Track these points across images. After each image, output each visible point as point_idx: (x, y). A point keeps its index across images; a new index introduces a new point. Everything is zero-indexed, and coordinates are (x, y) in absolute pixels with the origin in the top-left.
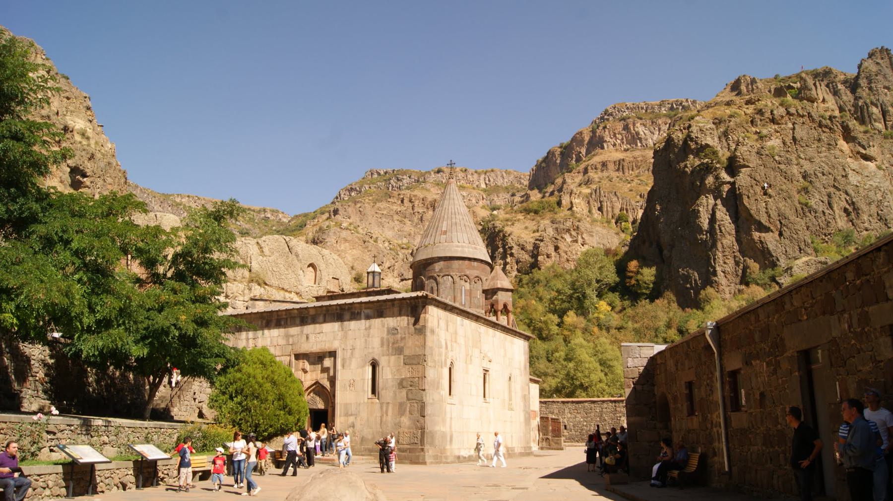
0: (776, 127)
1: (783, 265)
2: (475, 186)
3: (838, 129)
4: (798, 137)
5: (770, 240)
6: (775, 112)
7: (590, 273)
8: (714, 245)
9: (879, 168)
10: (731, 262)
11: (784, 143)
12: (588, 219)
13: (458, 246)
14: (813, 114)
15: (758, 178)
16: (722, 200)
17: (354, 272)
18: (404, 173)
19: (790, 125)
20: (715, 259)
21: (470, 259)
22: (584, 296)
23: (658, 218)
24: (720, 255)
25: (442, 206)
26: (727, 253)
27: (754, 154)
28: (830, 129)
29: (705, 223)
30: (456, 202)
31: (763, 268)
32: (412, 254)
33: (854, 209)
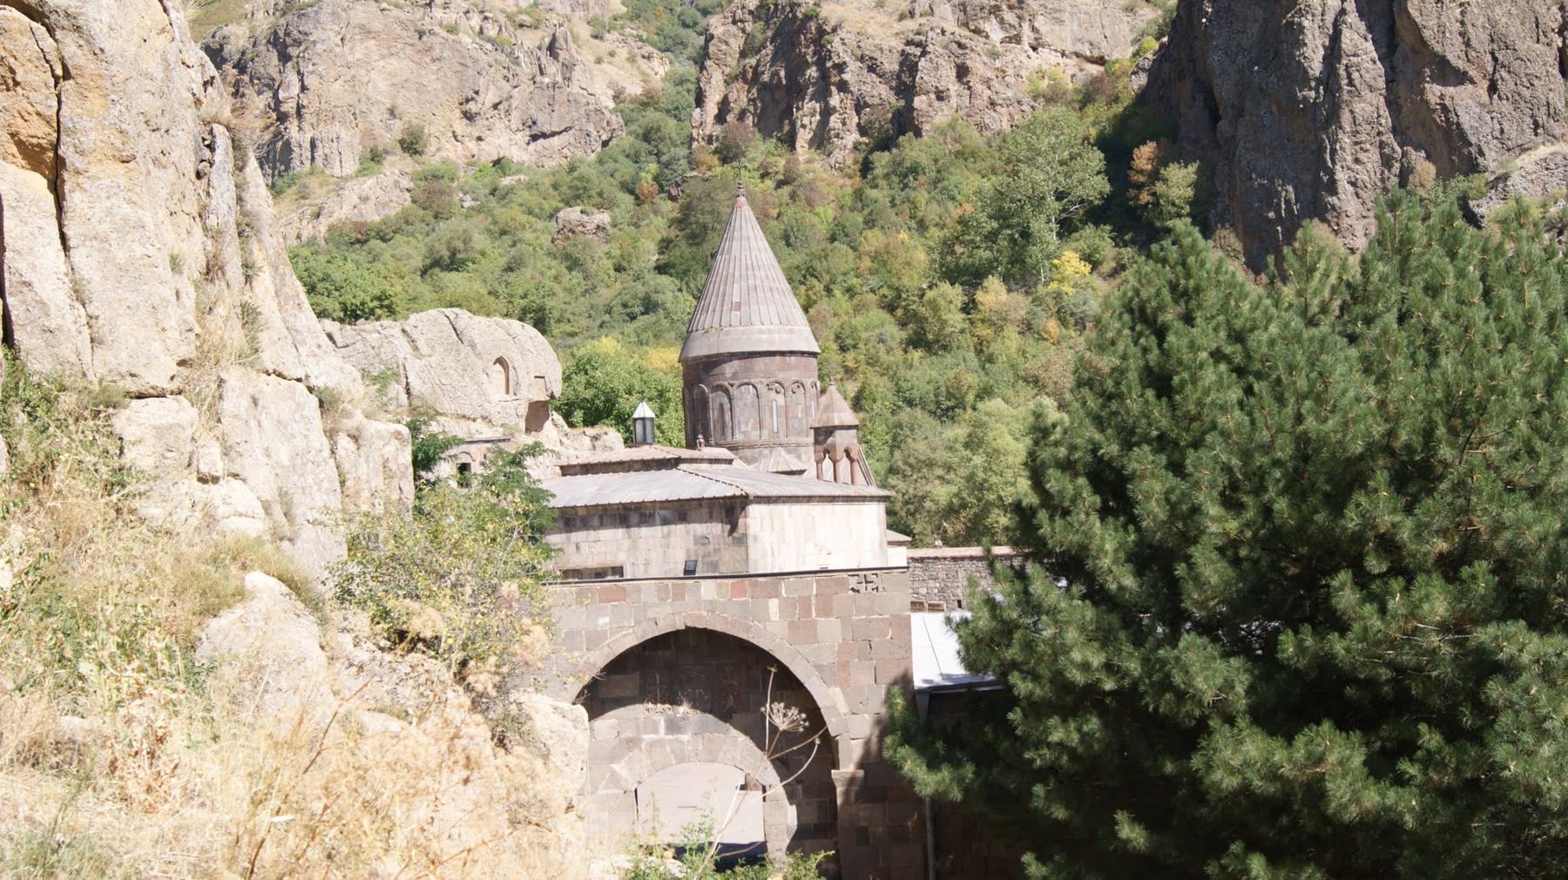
1: (1492, 166)
5: (1466, 104)
8: (1333, 117)
10: (1372, 158)
13: (761, 332)
17: (398, 125)
20: (1333, 152)
21: (783, 353)
22: (1026, 234)
24: (1346, 140)
25: (729, 252)
26: (1363, 137)
29: (1314, 57)
30: (753, 244)
31: (1444, 175)
32: (552, 49)
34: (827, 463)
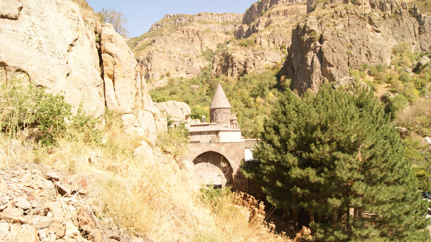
0: (342, 19)
2: (217, 22)
3: (367, 19)
4: (350, 24)
5: (333, 70)
6: (342, 13)
7: (266, 81)
8: (312, 72)
9: (382, 36)
11: (345, 26)
12: (268, 49)
14: (357, 13)
15: (331, 45)
16: (317, 53)
17: (166, 72)
18: (183, 16)
19: (348, 18)
22: (264, 90)
23: (293, 59)
24: (314, 76)
27: (330, 34)
28: (364, 19)
29: (309, 63)
31: (330, 81)
33: (370, 54)
34: (232, 125)
